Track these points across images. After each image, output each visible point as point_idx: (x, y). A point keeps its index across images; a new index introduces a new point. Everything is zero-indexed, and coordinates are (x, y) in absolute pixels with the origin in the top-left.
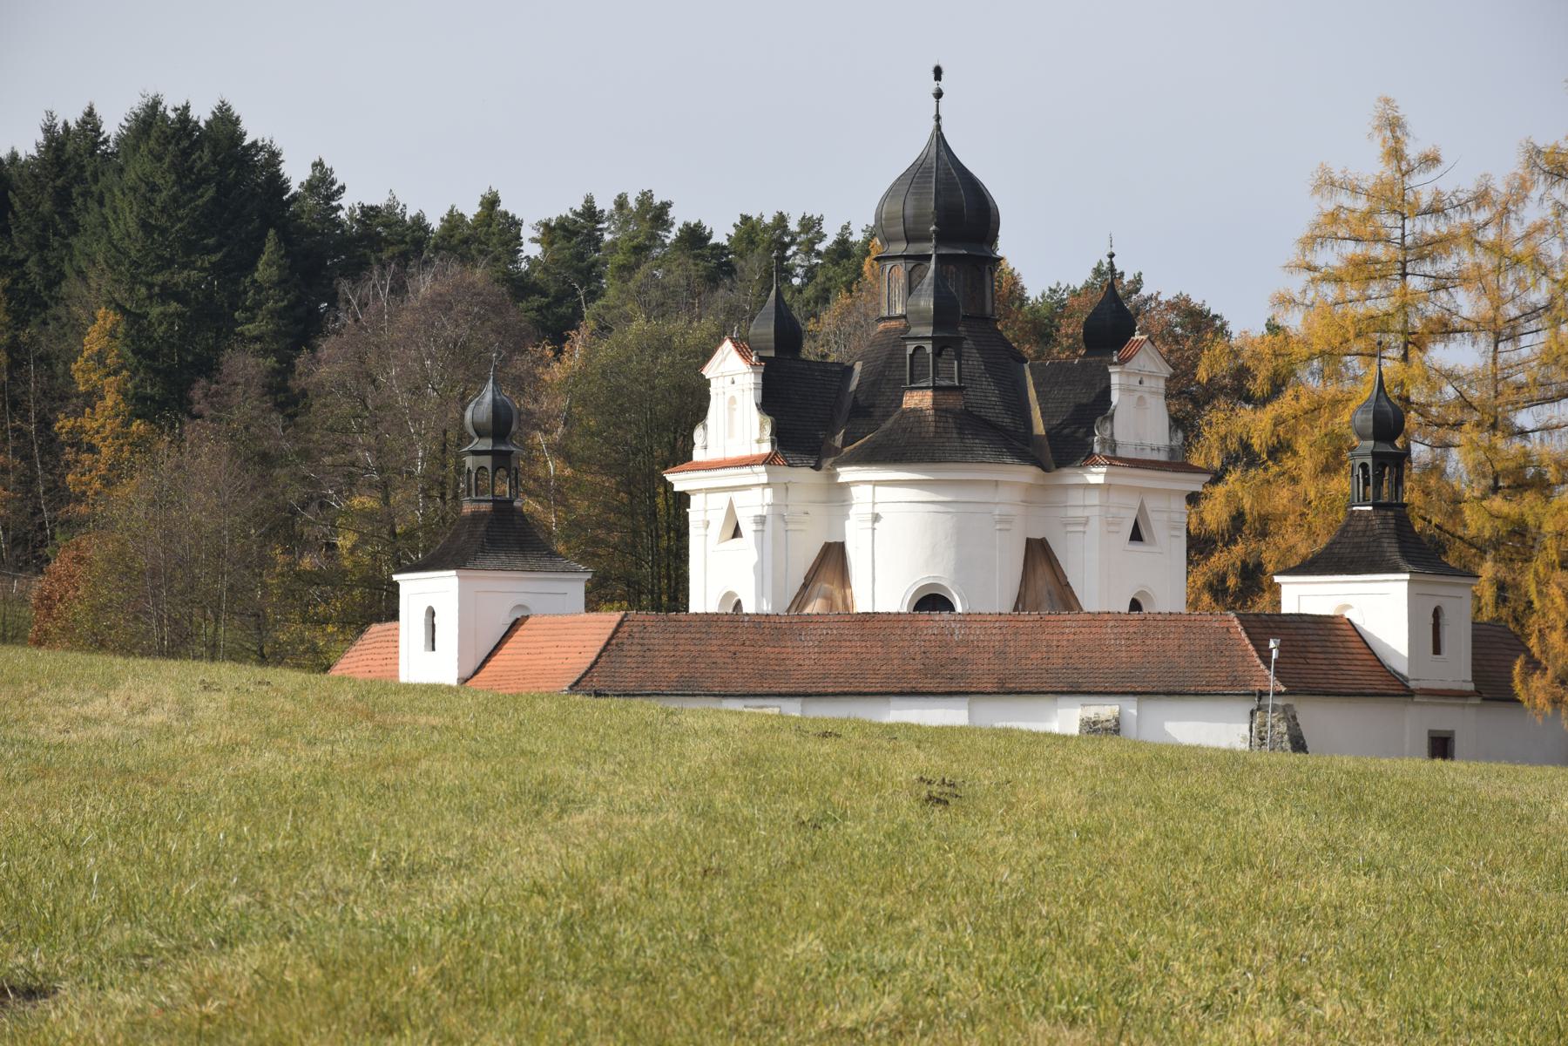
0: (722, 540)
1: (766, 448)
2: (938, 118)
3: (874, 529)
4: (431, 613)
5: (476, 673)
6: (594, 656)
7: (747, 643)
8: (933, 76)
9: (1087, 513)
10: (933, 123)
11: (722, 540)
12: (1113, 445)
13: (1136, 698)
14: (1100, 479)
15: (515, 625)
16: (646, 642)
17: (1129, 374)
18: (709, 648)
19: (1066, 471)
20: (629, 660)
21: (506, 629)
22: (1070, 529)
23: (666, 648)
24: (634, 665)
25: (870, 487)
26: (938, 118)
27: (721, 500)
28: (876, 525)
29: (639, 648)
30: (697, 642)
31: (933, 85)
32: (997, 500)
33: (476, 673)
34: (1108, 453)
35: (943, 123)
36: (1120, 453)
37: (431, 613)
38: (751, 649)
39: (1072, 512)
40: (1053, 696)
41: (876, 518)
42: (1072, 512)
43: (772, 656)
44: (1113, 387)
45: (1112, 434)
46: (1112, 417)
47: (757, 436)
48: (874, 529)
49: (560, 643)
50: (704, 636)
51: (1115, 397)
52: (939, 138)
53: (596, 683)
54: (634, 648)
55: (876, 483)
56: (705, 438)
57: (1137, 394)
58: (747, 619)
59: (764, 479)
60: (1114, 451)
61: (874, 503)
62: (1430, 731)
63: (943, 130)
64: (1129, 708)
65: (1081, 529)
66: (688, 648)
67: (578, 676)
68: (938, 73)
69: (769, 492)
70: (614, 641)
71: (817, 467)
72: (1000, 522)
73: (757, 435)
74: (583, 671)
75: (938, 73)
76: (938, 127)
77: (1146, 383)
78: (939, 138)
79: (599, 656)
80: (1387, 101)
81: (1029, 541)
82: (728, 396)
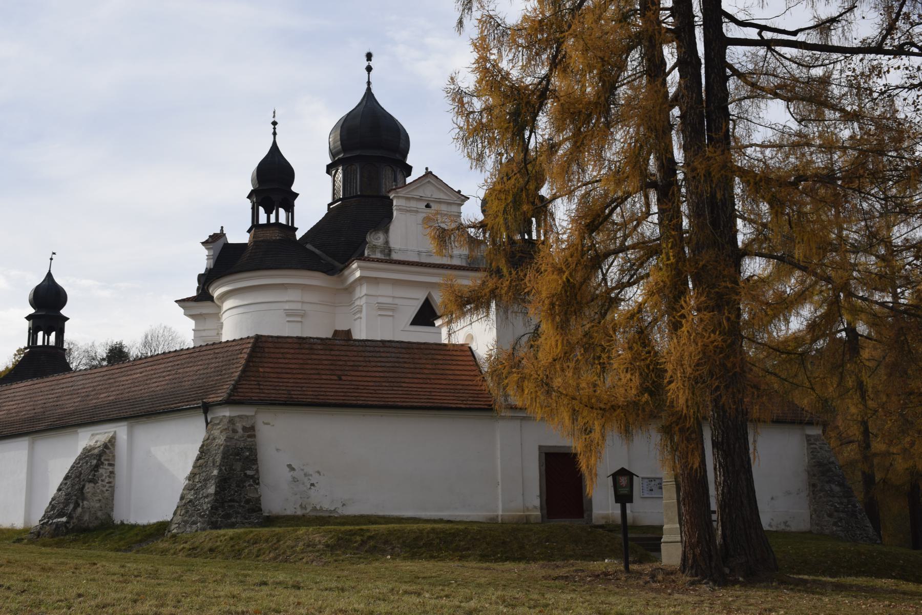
2: (369, 83)
8: (366, 59)
10: (366, 86)
12: (387, 250)
14: (358, 274)
17: (408, 199)
26: (369, 83)
32: (285, 299)
34: (379, 255)
35: (373, 87)
36: (395, 256)
45: (387, 242)
46: (387, 231)
51: (395, 213)
52: (369, 95)
57: (421, 217)
60: (389, 255)
62: (540, 447)
63: (374, 91)
64: (121, 431)
68: (369, 56)
72: (288, 315)
75: (369, 56)
76: (369, 89)
77: (434, 206)
78: (369, 95)
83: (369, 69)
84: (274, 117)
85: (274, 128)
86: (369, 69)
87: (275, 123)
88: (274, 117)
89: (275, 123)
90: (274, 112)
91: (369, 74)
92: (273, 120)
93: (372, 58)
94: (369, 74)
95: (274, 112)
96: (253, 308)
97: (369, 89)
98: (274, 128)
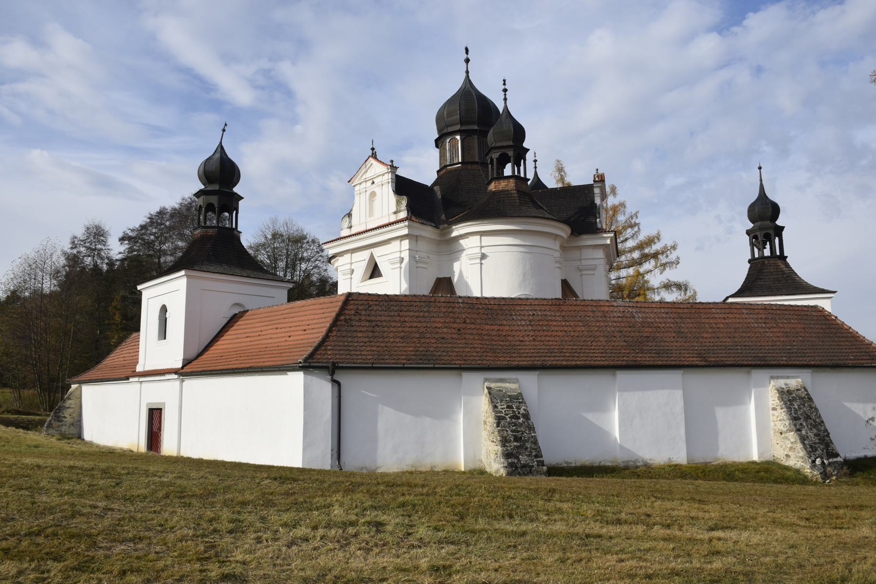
0: (363, 280)
1: (403, 214)
2: (467, 72)
3: (481, 264)
4: (164, 309)
5: (200, 354)
6: (321, 336)
7: (468, 321)
9: (594, 262)
10: (465, 75)
11: (363, 280)
13: (810, 371)
15: (233, 320)
16: (373, 318)
18: (435, 325)
19: (584, 236)
20: (360, 335)
21: (225, 321)
22: (584, 272)
23: (394, 324)
24: (366, 340)
25: (479, 237)
26: (467, 72)
27: (365, 255)
28: (483, 261)
29: (367, 324)
30: (422, 320)
31: (465, 56)
33: (200, 354)
37: (164, 309)
38: (473, 326)
39: (584, 263)
40: (747, 369)
41: (483, 257)
42: (584, 263)
43: (494, 333)
44: (595, 195)
47: (394, 209)
48: (481, 264)
49: (278, 326)
50: (426, 314)
52: (468, 80)
53: (329, 355)
54: (363, 324)
55: (482, 234)
56: (350, 222)
58: (460, 301)
59: (405, 231)
61: (481, 247)
65: (592, 272)
66: (415, 324)
67: (311, 349)
69: (406, 244)
70: (342, 318)
71: (437, 227)
73: (394, 208)
74: (315, 345)
76: (468, 76)
78: (468, 80)
79: (330, 330)
80: (558, 161)
81: (562, 280)
82: (368, 193)
83: (467, 61)
84: (504, 84)
85: (505, 95)
86: (467, 61)
87: (505, 90)
88: (504, 84)
89: (505, 90)
90: (504, 81)
91: (467, 64)
92: (503, 87)
93: (469, 53)
94: (467, 64)
95: (504, 81)
96: (515, 248)
97: (468, 76)
98: (505, 95)
